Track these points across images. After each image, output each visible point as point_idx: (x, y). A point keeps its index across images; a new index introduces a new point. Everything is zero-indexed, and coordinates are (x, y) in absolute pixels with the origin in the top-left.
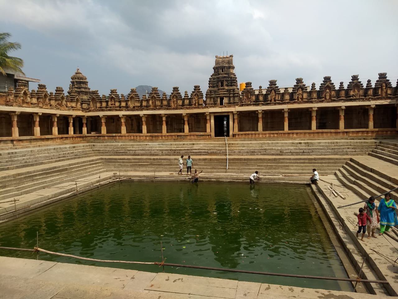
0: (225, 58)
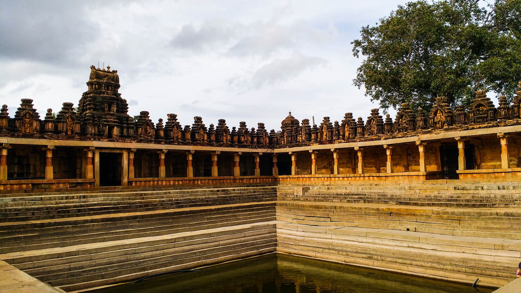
0: (106, 72)
